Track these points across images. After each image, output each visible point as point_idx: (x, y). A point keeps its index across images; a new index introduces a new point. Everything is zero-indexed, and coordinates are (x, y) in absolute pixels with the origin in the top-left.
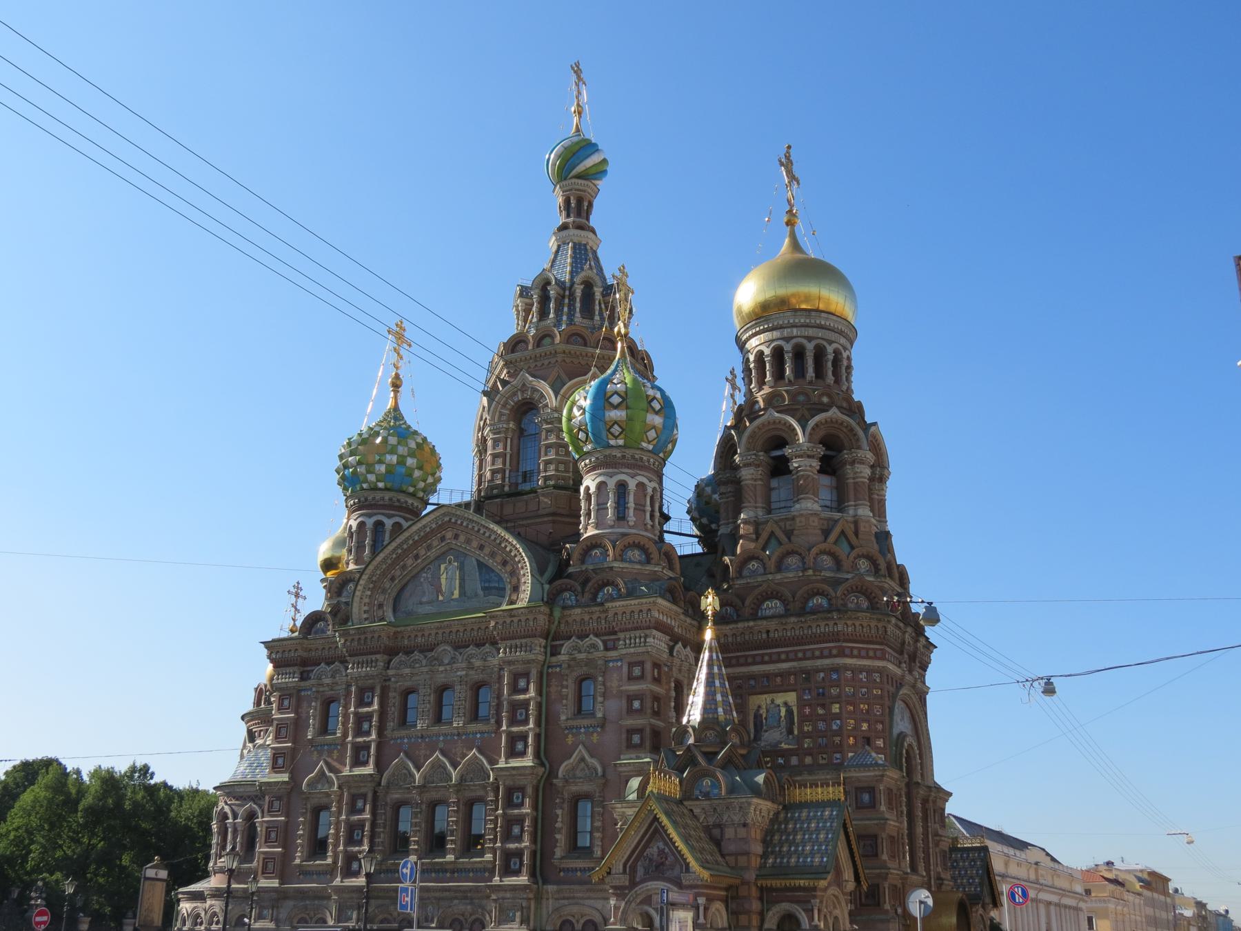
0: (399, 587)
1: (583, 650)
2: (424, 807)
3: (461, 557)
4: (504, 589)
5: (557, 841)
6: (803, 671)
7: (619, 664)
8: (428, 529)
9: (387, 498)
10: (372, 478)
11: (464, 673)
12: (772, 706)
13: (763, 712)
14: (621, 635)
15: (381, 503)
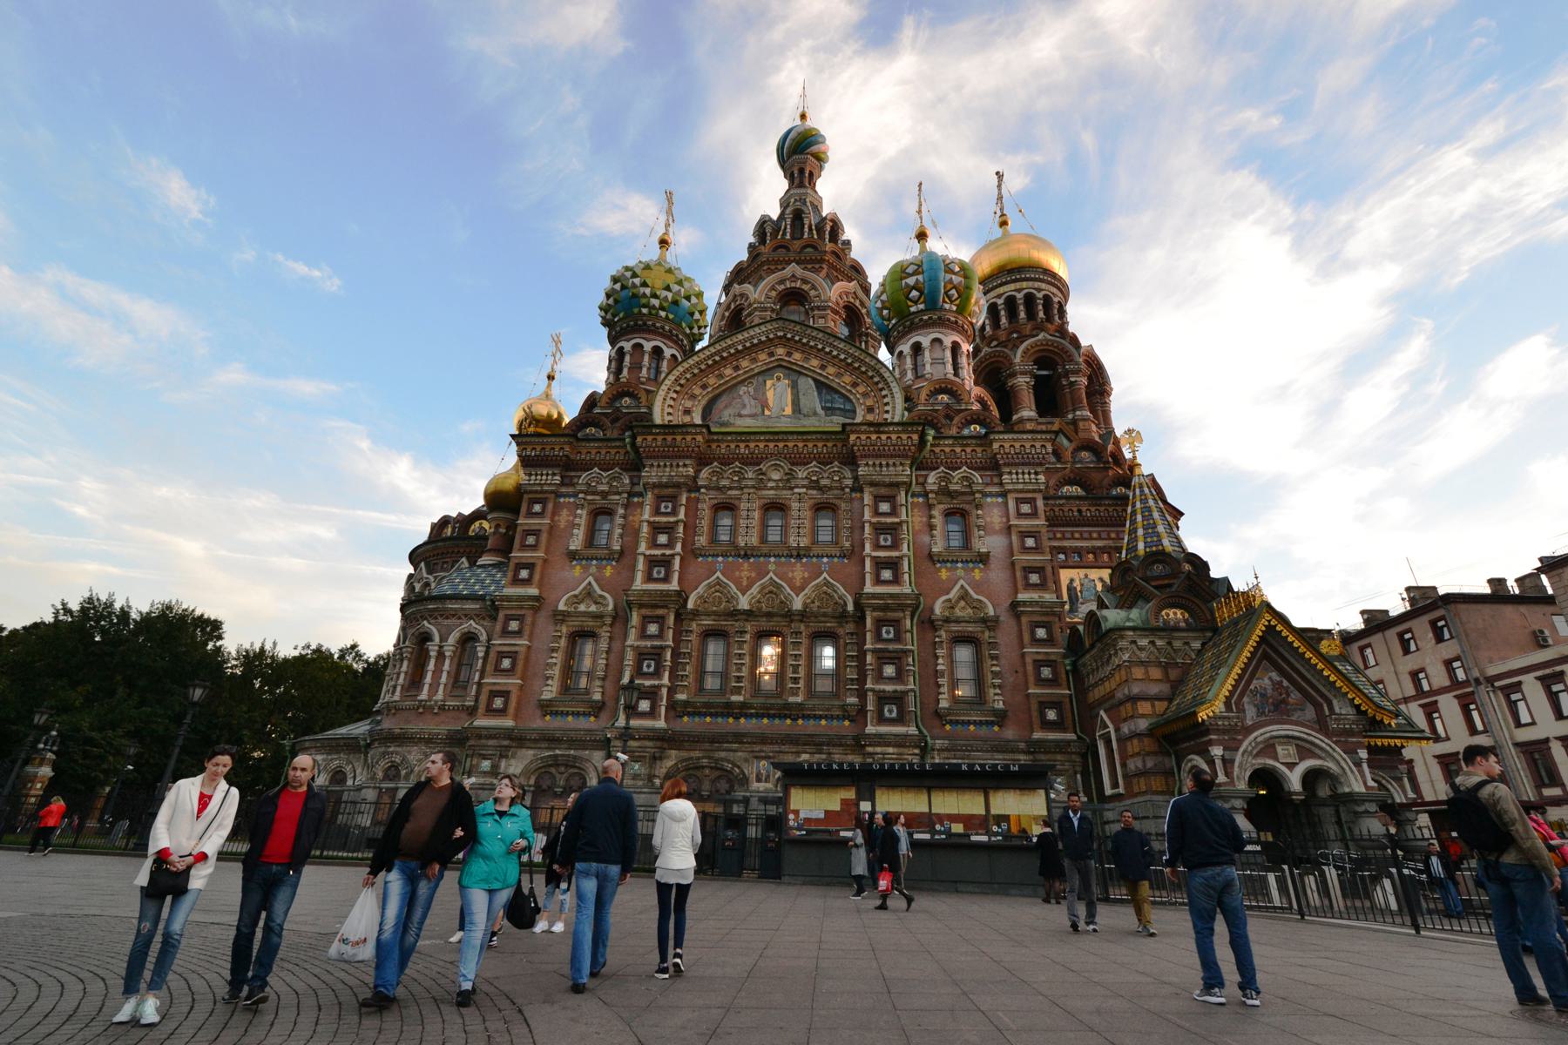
0: (711, 396)
2: (747, 637)
3: (794, 372)
4: (854, 412)
5: (939, 686)
7: (1000, 500)
8: (755, 341)
9: (667, 328)
11: (804, 490)
12: (1086, 580)
13: (1077, 584)
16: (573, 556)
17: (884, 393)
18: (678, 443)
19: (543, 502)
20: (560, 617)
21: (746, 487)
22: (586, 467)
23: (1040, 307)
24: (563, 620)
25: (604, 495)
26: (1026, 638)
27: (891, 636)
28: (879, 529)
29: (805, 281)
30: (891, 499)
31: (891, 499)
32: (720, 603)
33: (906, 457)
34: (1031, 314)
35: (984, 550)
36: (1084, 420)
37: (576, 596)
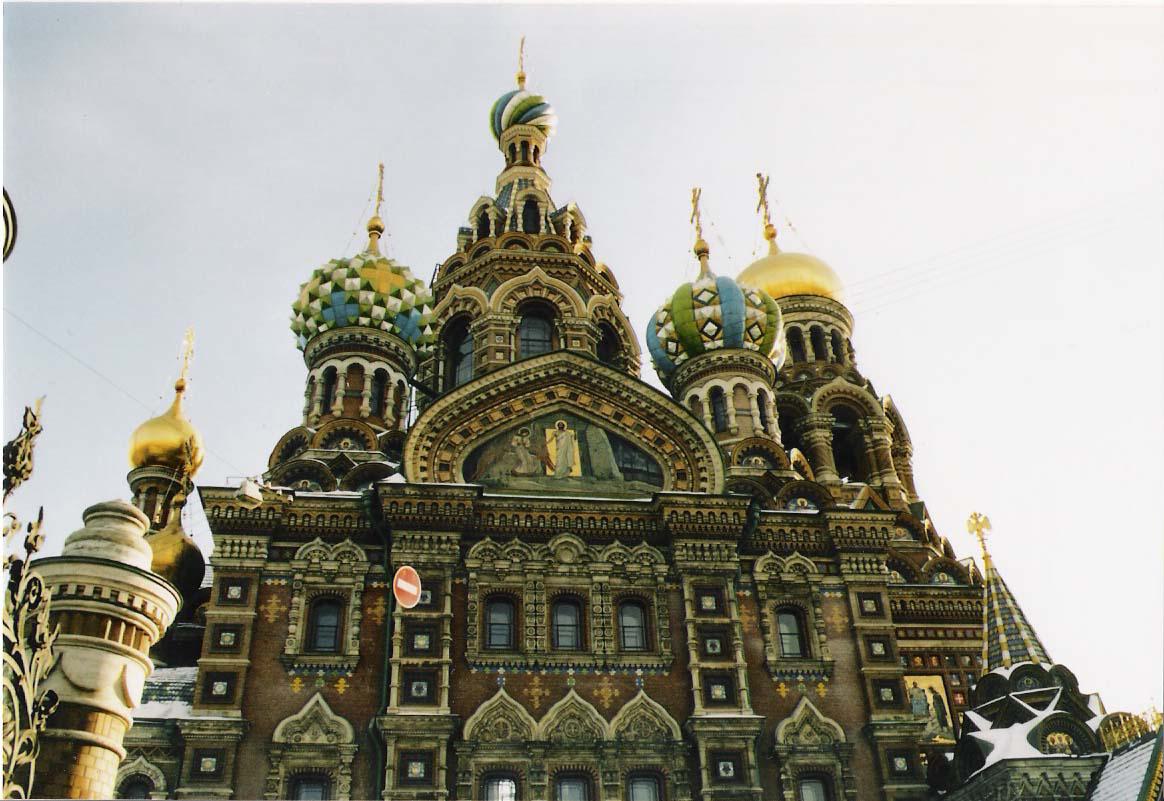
0: (475, 445)
1: (787, 569)
2: (546, 779)
4: (661, 476)
6: (948, 652)
7: (839, 595)
8: (532, 377)
9: (393, 345)
10: (378, 311)
11: (606, 578)
12: (916, 690)
14: (845, 557)
15: (384, 348)
16: (287, 663)
17: (698, 455)
18: (441, 510)
19: (244, 584)
20: (278, 752)
21: (531, 571)
22: (306, 536)
23: (829, 344)
24: (281, 757)
25: (331, 577)
26: (885, 771)
27: (731, 774)
28: (704, 632)
29: (553, 291)
30: (717, 592)
31: (717, 592)
32: (506, 733)
33: (732, 539)
34: (820, 354)
35: (828, 659)
36: (893, 488)
37: (298, 722)
